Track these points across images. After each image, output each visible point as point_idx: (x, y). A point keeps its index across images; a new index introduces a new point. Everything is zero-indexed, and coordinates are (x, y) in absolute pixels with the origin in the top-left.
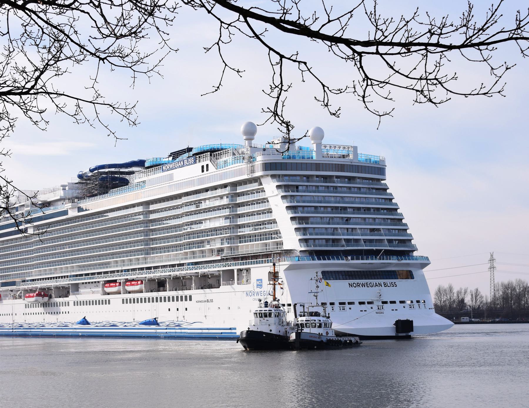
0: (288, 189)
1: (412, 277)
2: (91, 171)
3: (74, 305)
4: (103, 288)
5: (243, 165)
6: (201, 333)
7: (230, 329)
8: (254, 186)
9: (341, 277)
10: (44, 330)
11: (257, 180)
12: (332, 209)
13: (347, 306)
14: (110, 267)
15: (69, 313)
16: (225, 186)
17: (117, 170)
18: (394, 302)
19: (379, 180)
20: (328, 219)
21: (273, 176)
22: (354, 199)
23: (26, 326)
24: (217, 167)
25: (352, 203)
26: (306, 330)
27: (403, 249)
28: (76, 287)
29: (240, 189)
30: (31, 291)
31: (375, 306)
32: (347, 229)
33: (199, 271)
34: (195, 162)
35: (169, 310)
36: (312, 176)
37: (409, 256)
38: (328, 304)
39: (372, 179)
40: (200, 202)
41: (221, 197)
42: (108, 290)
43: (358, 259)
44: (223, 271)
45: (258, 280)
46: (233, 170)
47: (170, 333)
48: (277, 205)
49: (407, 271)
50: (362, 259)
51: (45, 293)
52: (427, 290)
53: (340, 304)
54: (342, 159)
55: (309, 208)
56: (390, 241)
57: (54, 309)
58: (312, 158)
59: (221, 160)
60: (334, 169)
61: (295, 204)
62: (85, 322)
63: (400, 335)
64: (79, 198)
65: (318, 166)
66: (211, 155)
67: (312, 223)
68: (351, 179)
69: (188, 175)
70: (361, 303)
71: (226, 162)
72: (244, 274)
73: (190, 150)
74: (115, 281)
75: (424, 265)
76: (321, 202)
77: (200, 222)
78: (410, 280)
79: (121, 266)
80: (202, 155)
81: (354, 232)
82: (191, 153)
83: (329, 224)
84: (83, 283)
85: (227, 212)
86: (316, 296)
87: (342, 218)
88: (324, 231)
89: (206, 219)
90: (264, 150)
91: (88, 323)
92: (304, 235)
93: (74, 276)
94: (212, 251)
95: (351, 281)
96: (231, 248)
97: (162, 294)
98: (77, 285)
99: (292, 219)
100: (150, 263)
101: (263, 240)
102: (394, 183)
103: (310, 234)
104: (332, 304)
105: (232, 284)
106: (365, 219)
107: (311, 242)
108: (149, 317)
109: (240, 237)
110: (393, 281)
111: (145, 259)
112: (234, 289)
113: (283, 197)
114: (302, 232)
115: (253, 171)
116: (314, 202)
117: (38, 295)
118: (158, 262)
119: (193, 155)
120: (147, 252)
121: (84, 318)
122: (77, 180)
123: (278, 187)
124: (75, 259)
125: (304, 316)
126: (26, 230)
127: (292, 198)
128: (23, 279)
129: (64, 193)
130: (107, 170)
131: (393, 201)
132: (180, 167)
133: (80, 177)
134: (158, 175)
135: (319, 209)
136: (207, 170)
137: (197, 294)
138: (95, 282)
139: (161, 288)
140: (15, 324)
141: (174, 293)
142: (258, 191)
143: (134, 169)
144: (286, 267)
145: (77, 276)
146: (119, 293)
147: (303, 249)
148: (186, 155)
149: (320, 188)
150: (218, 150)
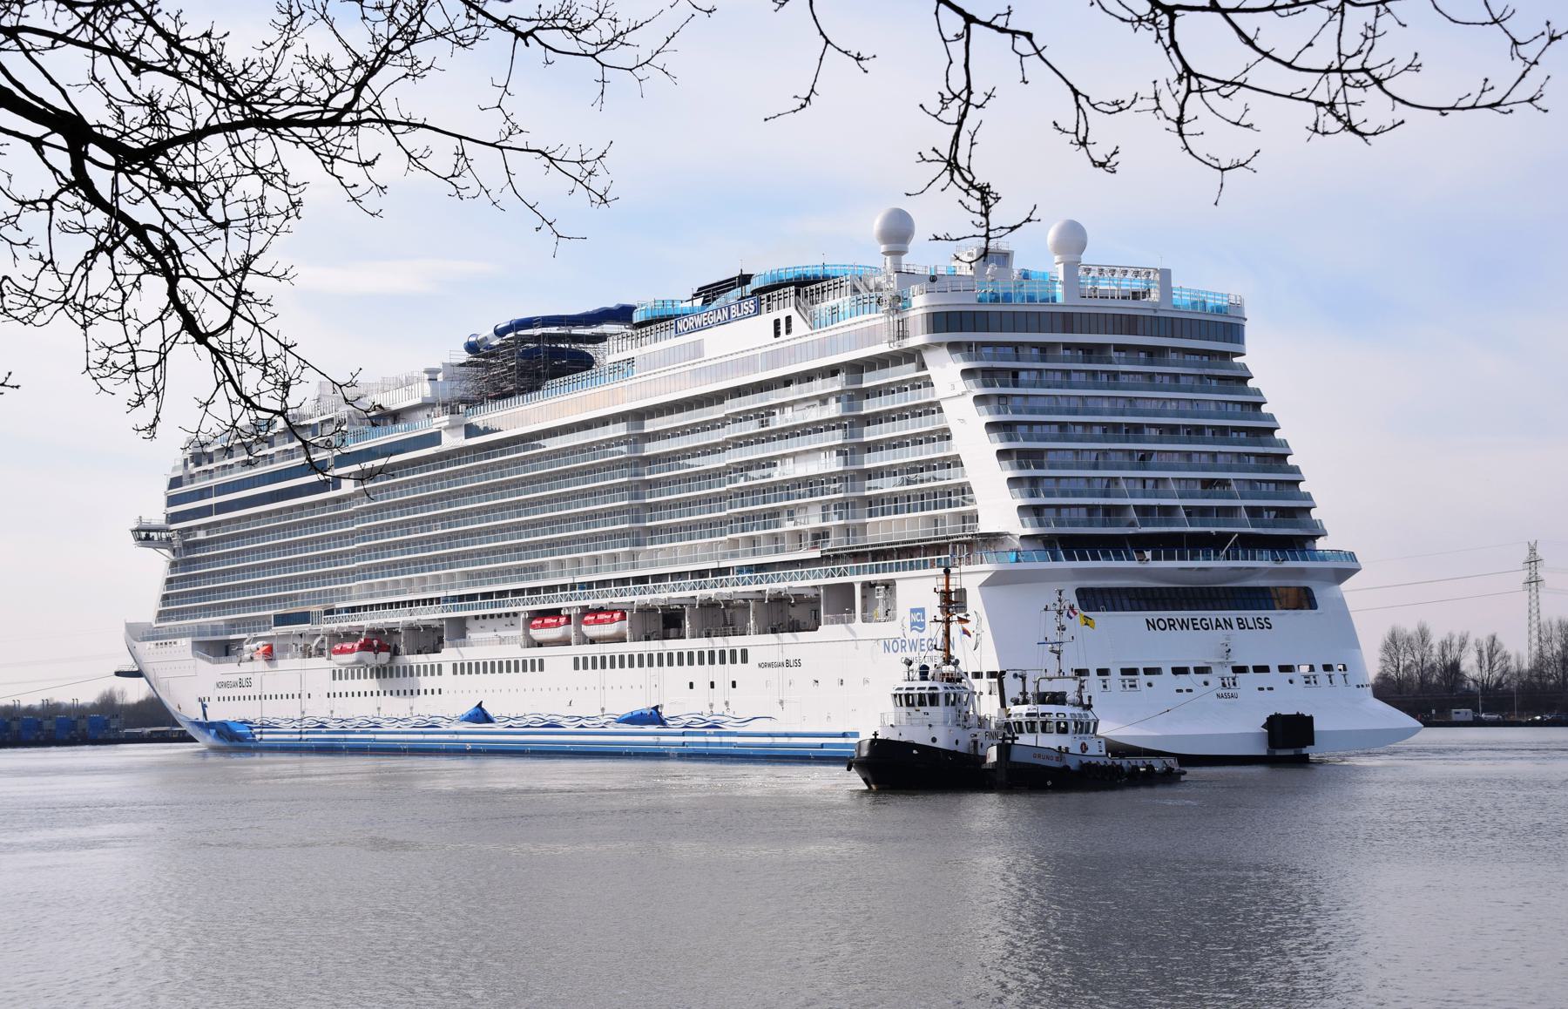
0: (992, 378)
1: (1312, 605)
2: (499, 333)
3: (455, 672)
4: (526, 630)
5: (878, 319)
6: (770, 746)
7: (844, 735)
8: (907, 372)
9: (1126, 602)
10: (379, 737)
11: (913, 356)
12: (1105, 431)
13: (1142, 679)
14: (545, 577)
15: (443, 694)
16: (833, 371)
17: (563, 331)
18: (1265, 669)
19: (1226, 356)
20: (1094, 455)
21: (954, 347)
22: (1162, 404)
23: (333, 726)
24: (813, 322)
25: (1157, 414)
26: (1025, 739)
27: (1288, 530)
28: (460, 629)
29: (870, 380)
30: (348, 636)
31: (1214, 680)
32: (1144, 480)
33: (765, 587)
34: (758, 311)
35: (691, 685)
36: (1054, 345)
37: (1303, 549)
38: (1093, 673)
39: (1210, 354)
40: (769, 411)
41: (823, 400)
42: (539, 634)
43: (1169, 557)
44: (826, 587)
45: (913, 611)
46: (855, 331)
47: (693, 743)
48: (962, 421)
49: (1299, 589)
50: (1182, 558)
51: (381, 642)
52: (1352, 641)
53: (1125, 672)
54: (1131, 303)
55: (1046, 428)
56: (1254, 512)
57: (404, 683)
58: (1054, 299)
59: (823, 305)
60: (1110, 327)
61: (1010, 417)
62: (480, 715)
63: (1279, 753)
64: (471, 403)
65: (1067, 321)
66: (797, 293)
67: (1052, 466)
68: (1153, 353)
69: (741, 344)
70: (1177, 671)
71: (834, 311)
72: (880, 594)
73: (745, 279)
74: (556, 613)
75: (1342, 575)
76: (1075, 412)
77: (770, 463)
78: (1306, 614)
79: (571, 574)
81: (1161, 488)
82: (749, 289)
83: (1096, 467)
84: (477, 617)
85: (836, 438)
86: (1058, 653)
87: (1131, 452)
88: (1083, 485)
89: (784, 456)
90: (933, 279)
91: (487, 719)
92: (1032, 496)
93: (454, 599)
94: (799, 536)
95: (1154, 615)
96: (846, 529)
97: (673, 645)
98: (463, 620)
100: (644, 566)
102: (1266, 361)
103: (1048, 494)
104: (1103, 672)
105: (851, 621)
106: (1189, 454)
107: (1049, 515)
108: (642, 705)
109: (870, 501)
110: (1262, 614)
111: (633, 555)
112: (853, 633)
113: (979, 400)
114: (1027, 488)
115: (902, 334)
116: (1059, 413)
117: (363, 647)
118: (664, 564)
119: (754, 292)
120: (638, 538)
121: (480, 705)
122: (465, 357)
123: (966, 373)
124: (457, 556)
125: (1025, 702)
126: (336, 482)
127: (1003, 401)
128: (329, 605)
129: (433, 390)
130: (538, 331)
131: (1264, 409)
132: (719, 323)
133: (472, 348)
134: (668, 342)
135: (1071, 431)
136: (788, 332)
137: (761, 645)
138: (507, 615)
139: (673, 631)
140: (307, 721)
141: (703, 644)
142: (916, 384)
143: (607, 328)
144: (988, 575)
145: (461, 598)
146: (566, 642)
147: (1029, 531)
148: (736, 293)
149: (1075, 377)
150: (816, 280)
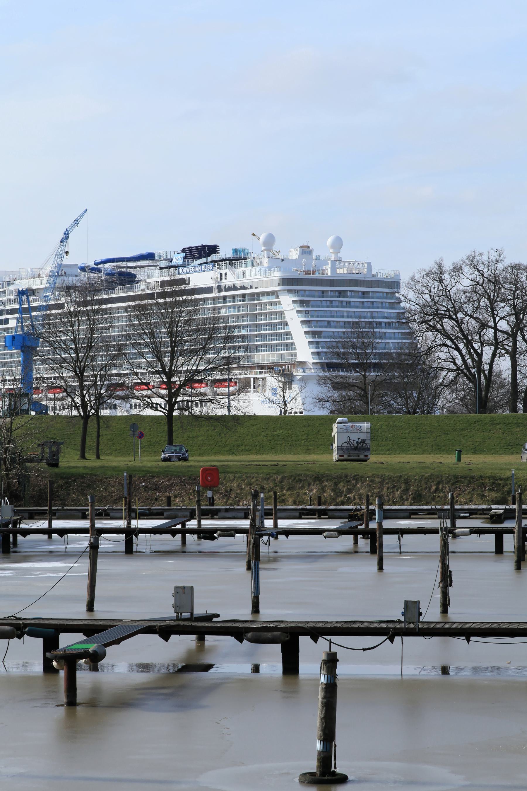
8: (272, 299)
12: (345, 324)
21: (289, 291)
24: (236, 275)
58: (327, 274)
65: (331, 282)
66: (230, 264)
72: (260, 382)
80: (221, 263)
99: (306, 333)
101: (279, 351)
107: (323, 355)
113: (298, 312)
114: (315, 345)
119: (211, 262)
123: (294, 302)
126: (7, 321)
127: (307, 312)
136: (226, 279)
142: (276, 303)
